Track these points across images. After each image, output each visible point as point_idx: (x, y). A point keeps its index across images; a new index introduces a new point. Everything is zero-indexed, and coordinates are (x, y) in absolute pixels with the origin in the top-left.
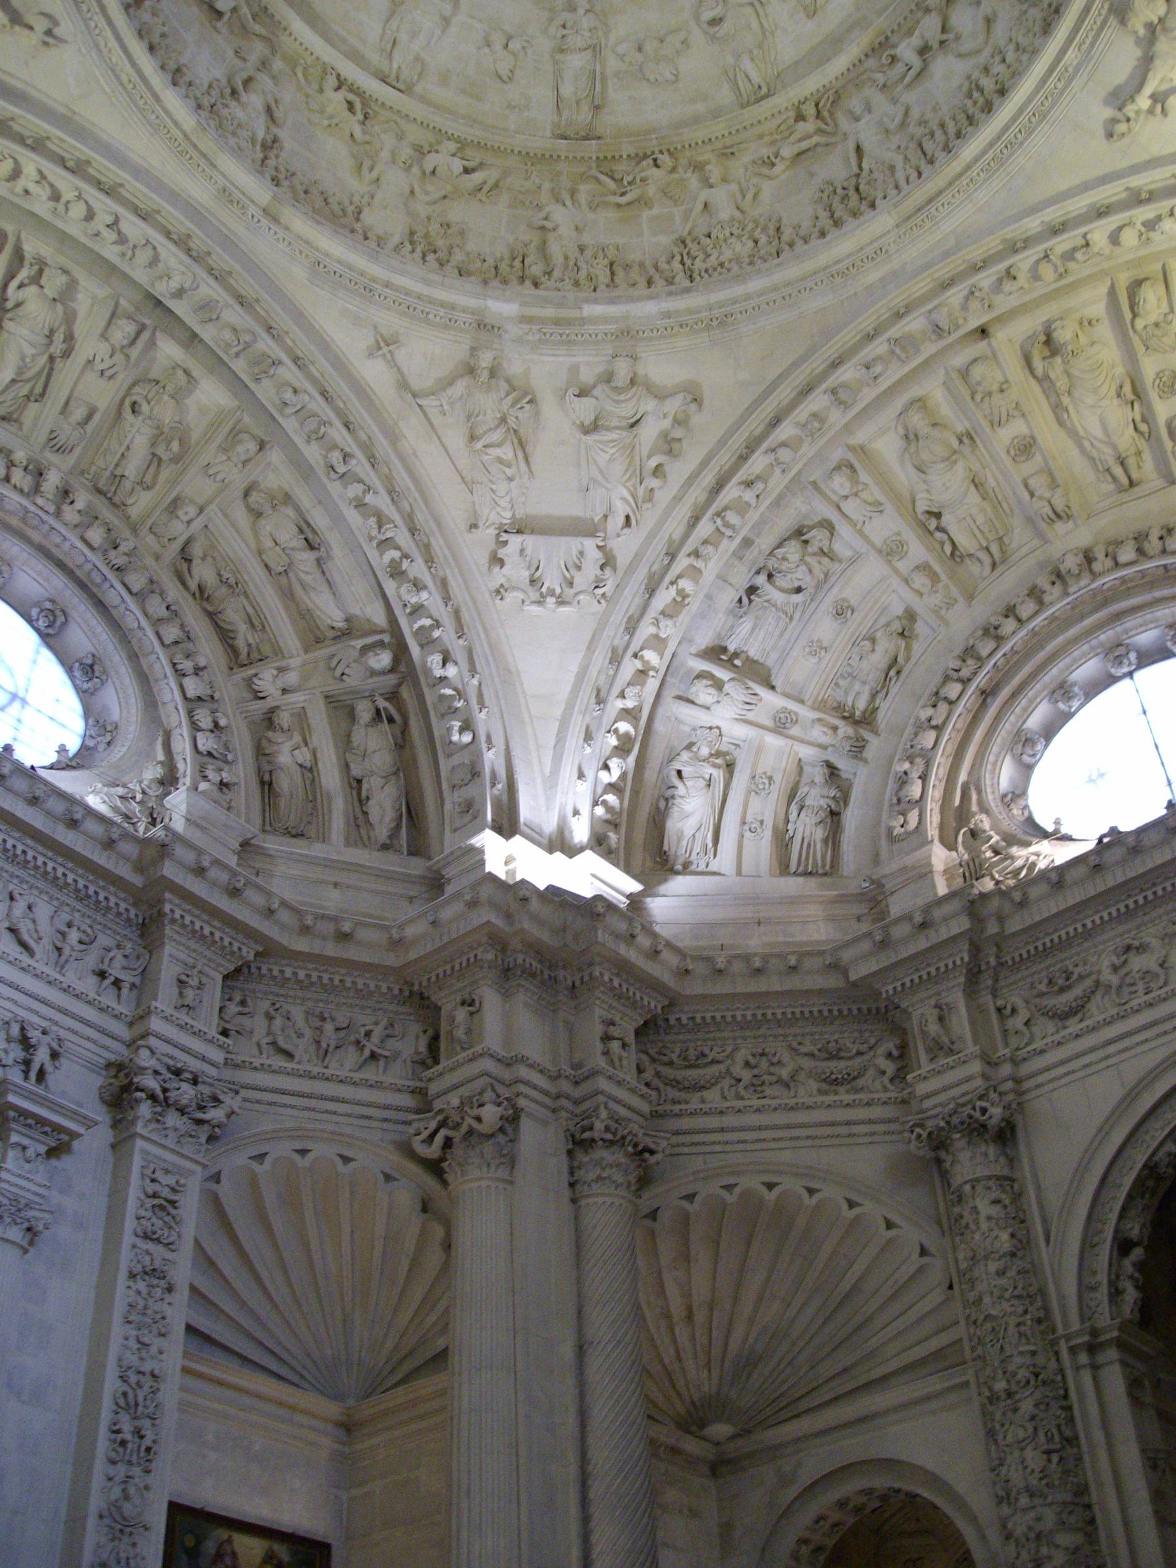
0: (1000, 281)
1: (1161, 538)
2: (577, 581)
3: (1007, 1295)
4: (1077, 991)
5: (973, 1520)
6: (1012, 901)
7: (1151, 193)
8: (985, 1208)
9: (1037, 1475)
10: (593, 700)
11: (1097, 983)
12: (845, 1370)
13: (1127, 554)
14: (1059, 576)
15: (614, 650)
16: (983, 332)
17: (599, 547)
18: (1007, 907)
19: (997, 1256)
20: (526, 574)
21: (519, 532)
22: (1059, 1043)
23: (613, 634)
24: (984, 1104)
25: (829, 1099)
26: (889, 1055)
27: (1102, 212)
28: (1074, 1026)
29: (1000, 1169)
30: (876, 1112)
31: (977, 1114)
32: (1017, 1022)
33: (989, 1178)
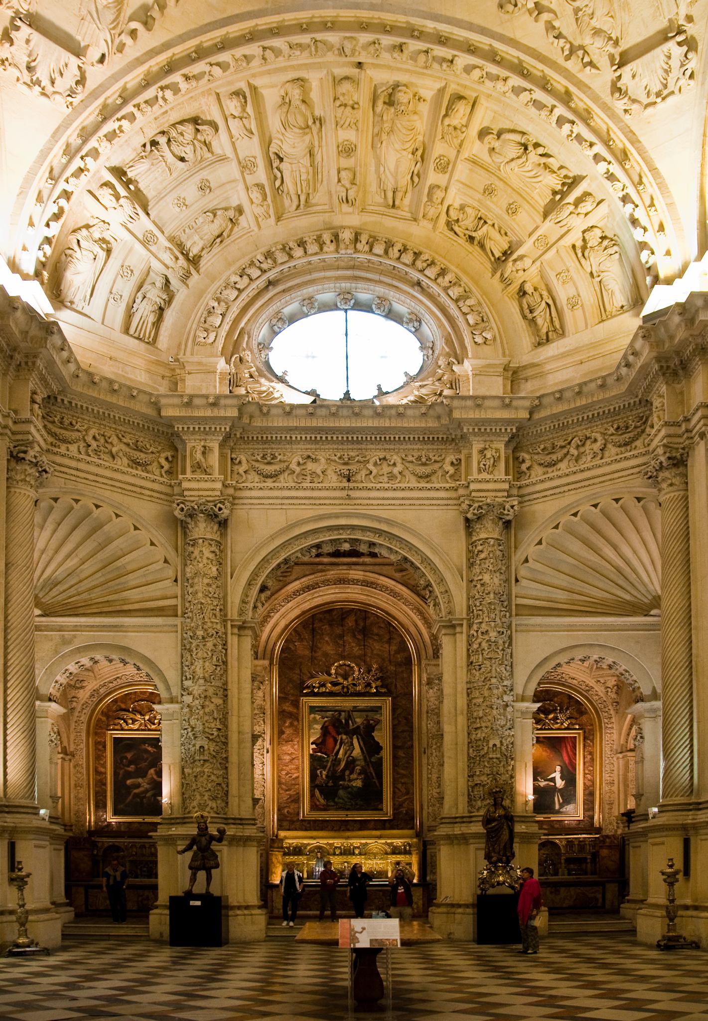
0: (394, 47)
2: (56, 82)
6: (261, 411)
7: (502, 59)
10: (47, 175)
11: (287, 467)
15: (68, 145)
16: (360, 65)
17: (79, 67)
18: (257, 413)
20: (26, 59)
21: (30, 25)
22: (261, 489)
23: (72, 135)
26: (167, 459)
27: (471, 49)
28: (269, 483)
32: (241, 470)
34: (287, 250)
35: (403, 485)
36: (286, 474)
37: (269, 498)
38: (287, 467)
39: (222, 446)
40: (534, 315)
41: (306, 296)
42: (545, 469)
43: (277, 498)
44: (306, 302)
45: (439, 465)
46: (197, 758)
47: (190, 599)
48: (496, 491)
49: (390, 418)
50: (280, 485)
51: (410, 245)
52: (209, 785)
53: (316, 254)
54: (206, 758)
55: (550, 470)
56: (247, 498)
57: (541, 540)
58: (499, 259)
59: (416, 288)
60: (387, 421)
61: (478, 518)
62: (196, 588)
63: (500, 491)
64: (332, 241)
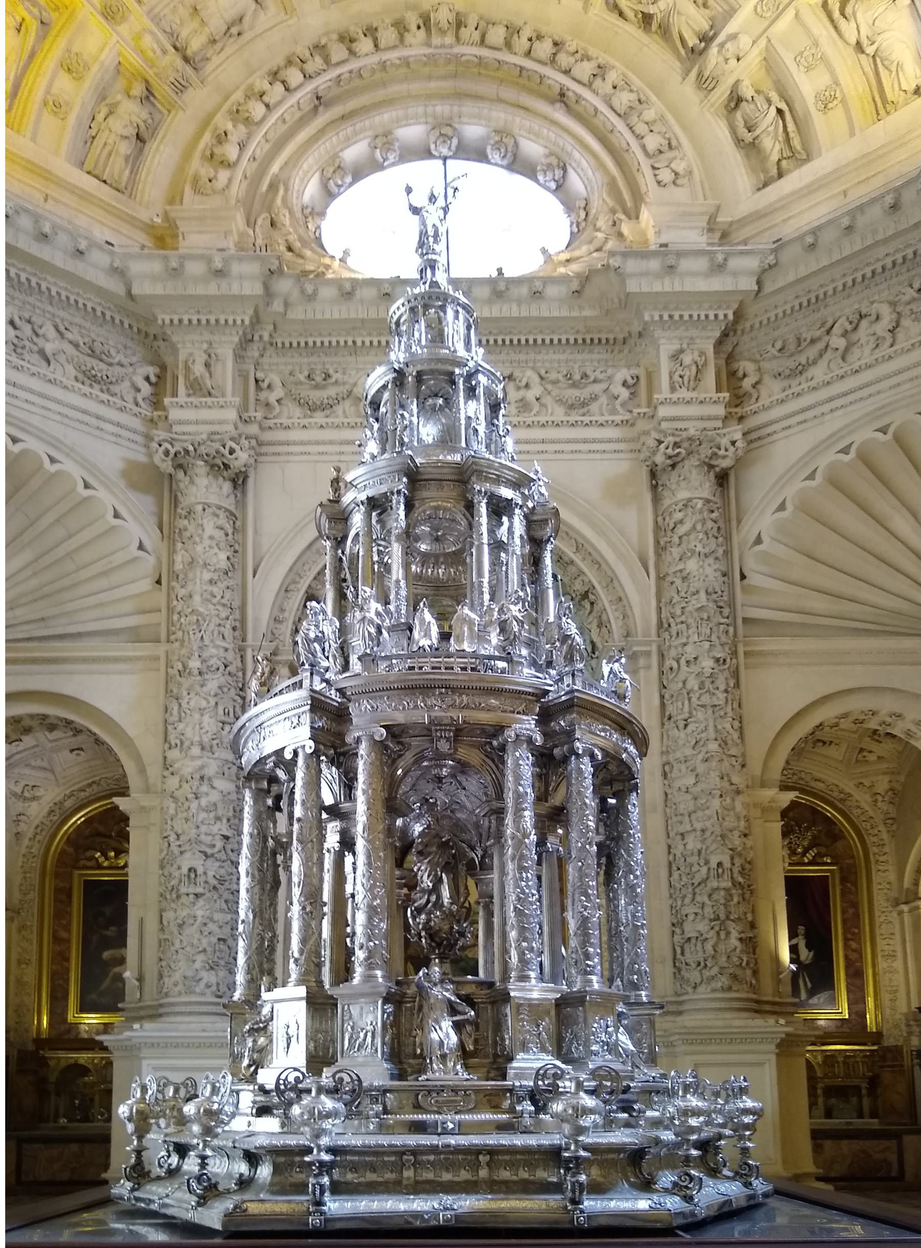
1: (530, 40)
3: (215, 601)
4: (332, 392)
5: (137, 757)
8: (210, 530)
9: (209, 735)
11: (350, 393)
12: (43, 619)
13: (497, 35)
14: (426, 22)
19: (212, 568)
24: (234, 445)
25: (86, 389)
26: (147, 379)
28: (319, 418)
29: (229, 504)
30: (124, 419)
31: (226, 452)
32: (272, 397)
33: (219, 508)
34: (347, 39)
35: (543, 419)
36: (347, 403)
37: (317, 443)
38: (350, 393)
39: (239, 357)
40: (757, 132)
41: (380, 131)
42: (786, 383)
43: (331, 443)
44: (379, 142)
45: (604, 386)
46: (183, 890)
47: (179, 608)
48: (702, 419)
49: (519, 302)
50: (336, 421)
51: (544, 30)
52: (205, 941)
53: (395, 47)
54: (199, 890)
55: (794, 382)
56: (281, 443)
57: (784, 502)
58: (693, 50)
59: (558, 105)
60: (515, 307)
61: (673, 466)
62: (190, 587)
63: (709, 418)
64: (419, 28)
